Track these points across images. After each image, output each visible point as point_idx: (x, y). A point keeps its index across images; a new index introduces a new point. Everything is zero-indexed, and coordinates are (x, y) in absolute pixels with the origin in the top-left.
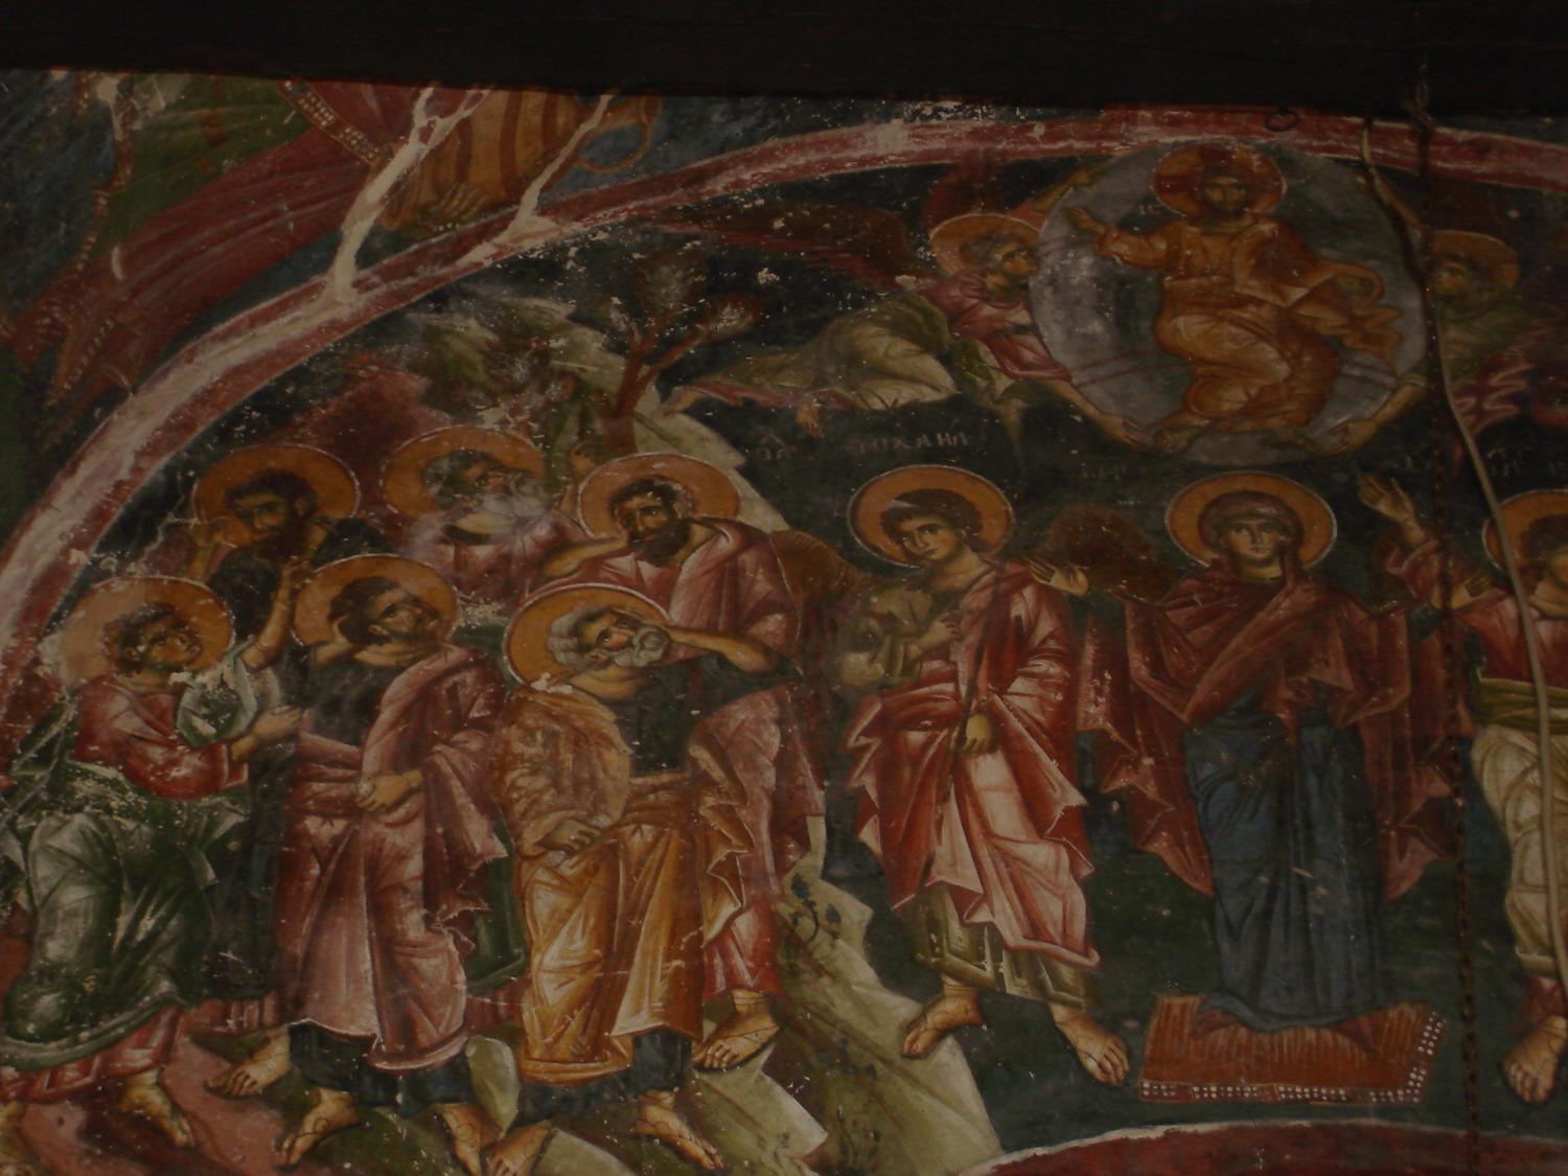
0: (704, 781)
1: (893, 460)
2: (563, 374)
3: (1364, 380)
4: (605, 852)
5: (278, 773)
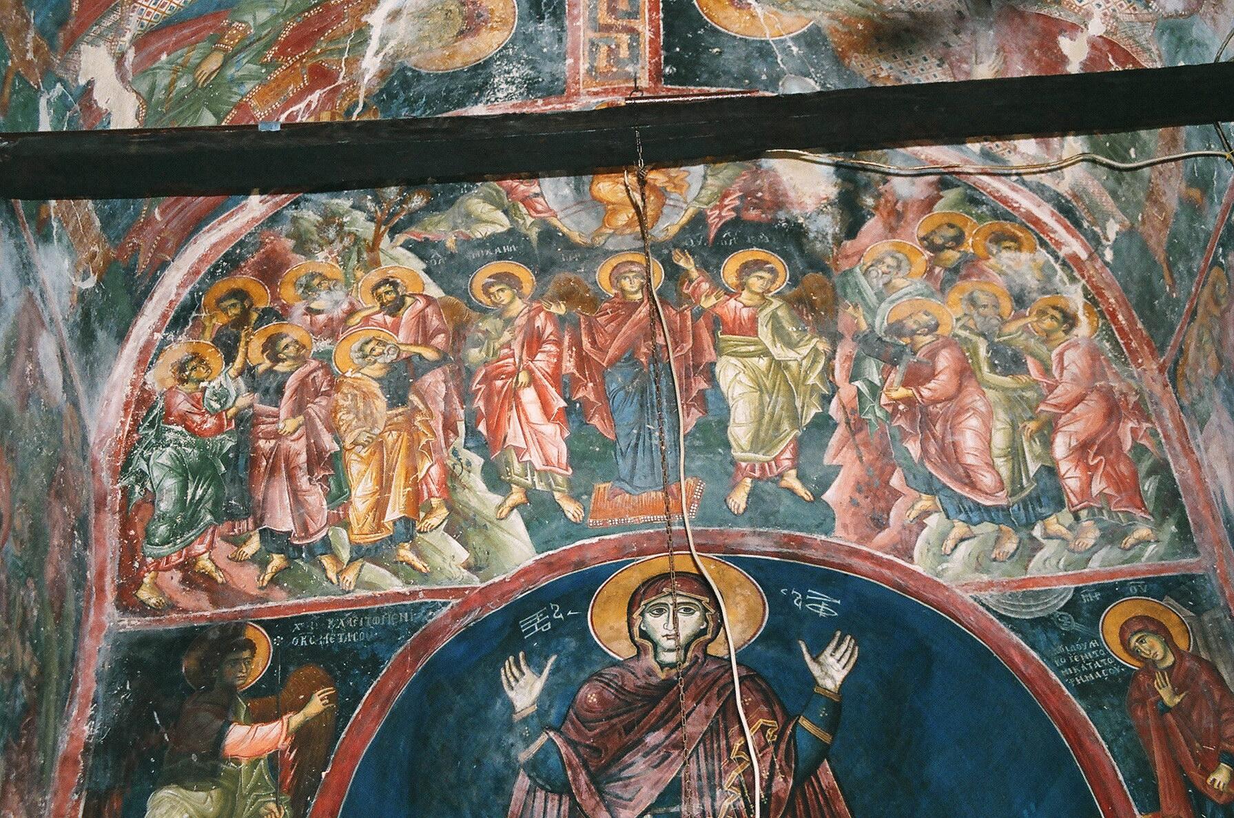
0: (416, 409)
1: (486, 260)
2: (349, 233)
3: (675, 206)
4: (378, 445)
5: (246, 422)
